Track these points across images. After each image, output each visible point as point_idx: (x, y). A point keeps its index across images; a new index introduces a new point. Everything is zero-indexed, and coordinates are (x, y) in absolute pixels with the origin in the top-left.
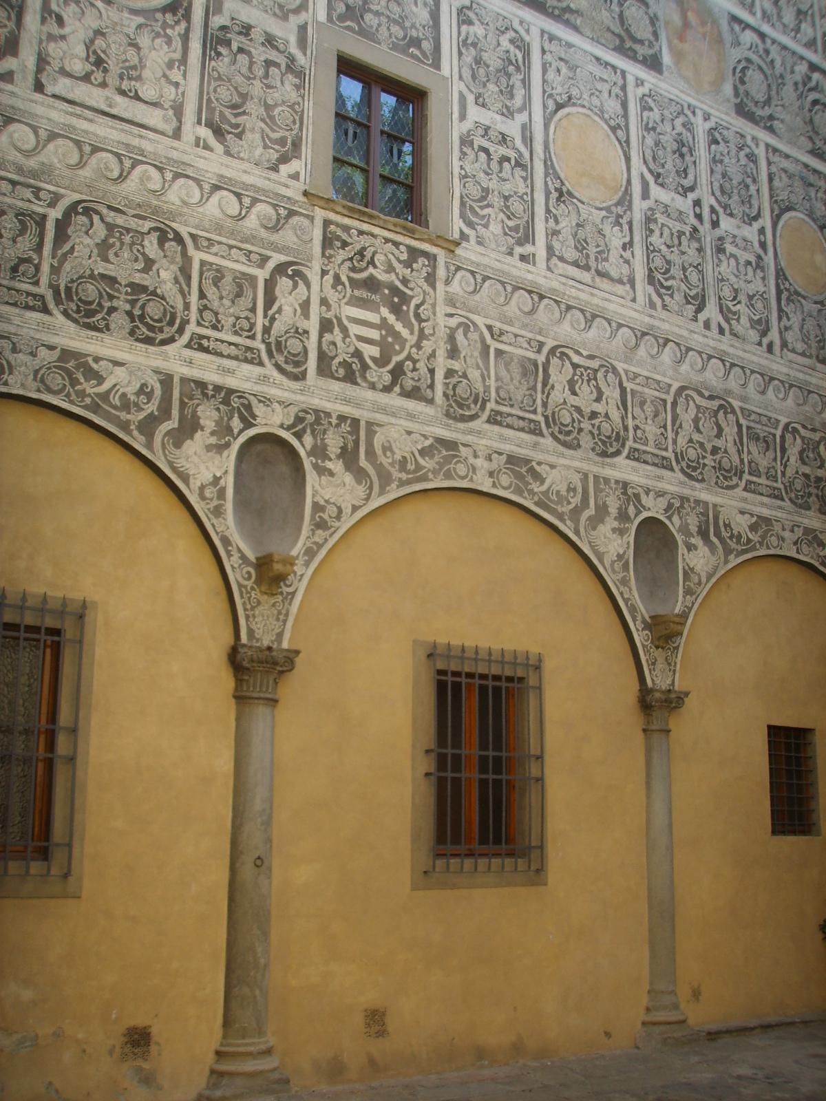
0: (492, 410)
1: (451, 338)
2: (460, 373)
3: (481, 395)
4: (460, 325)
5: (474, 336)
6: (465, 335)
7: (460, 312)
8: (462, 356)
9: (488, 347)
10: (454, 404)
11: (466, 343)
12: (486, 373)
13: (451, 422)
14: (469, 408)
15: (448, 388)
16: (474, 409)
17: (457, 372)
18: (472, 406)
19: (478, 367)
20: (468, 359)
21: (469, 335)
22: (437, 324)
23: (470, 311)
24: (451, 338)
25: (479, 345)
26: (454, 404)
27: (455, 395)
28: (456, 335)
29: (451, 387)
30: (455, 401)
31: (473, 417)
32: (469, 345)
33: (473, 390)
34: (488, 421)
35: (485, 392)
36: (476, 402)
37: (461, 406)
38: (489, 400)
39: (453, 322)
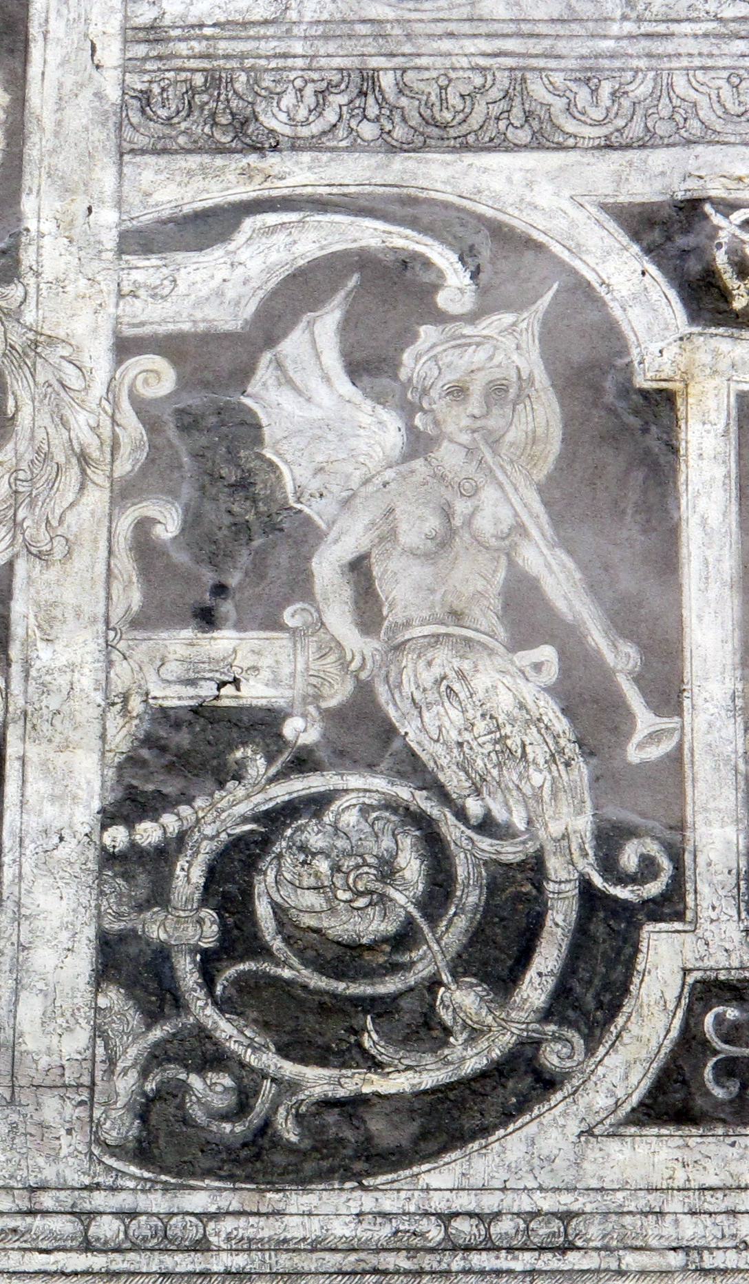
0: (707, 991)
1: (206, 429)
2: (300, 730)
3: (562, 879)
4: (299, 291)
5: (489, 347)
6: (369, 365)
7: (298, 173)
8: (326, 567)
9: (660, 405)
10: (225, 1029)
11: (382, 431)
12: (622, 660)
13: (198, 1201)
14: (427, 1031)
15: (159, 896)
16: (480, 1028)
17: (263, 725)
18: (464, 1000)
19: (526, 617)
20: (401, 586)
21: (425, 356)
22: (38, 343)
23: (436, 133)
24: (206, 429)
25: (544, 416)
26: (225, 1029)
27: (239, 937)
28: (267, 398)
29: (189, 875)
30: (249, 998)
31: (449, 1120)
32: (419, 444)
33: (470, 855)
34: (670, 1102)
35: (609, 839)
36: (497, 955)
37: (316, 1029)
38: (670, 906)
39: (216, 287)
